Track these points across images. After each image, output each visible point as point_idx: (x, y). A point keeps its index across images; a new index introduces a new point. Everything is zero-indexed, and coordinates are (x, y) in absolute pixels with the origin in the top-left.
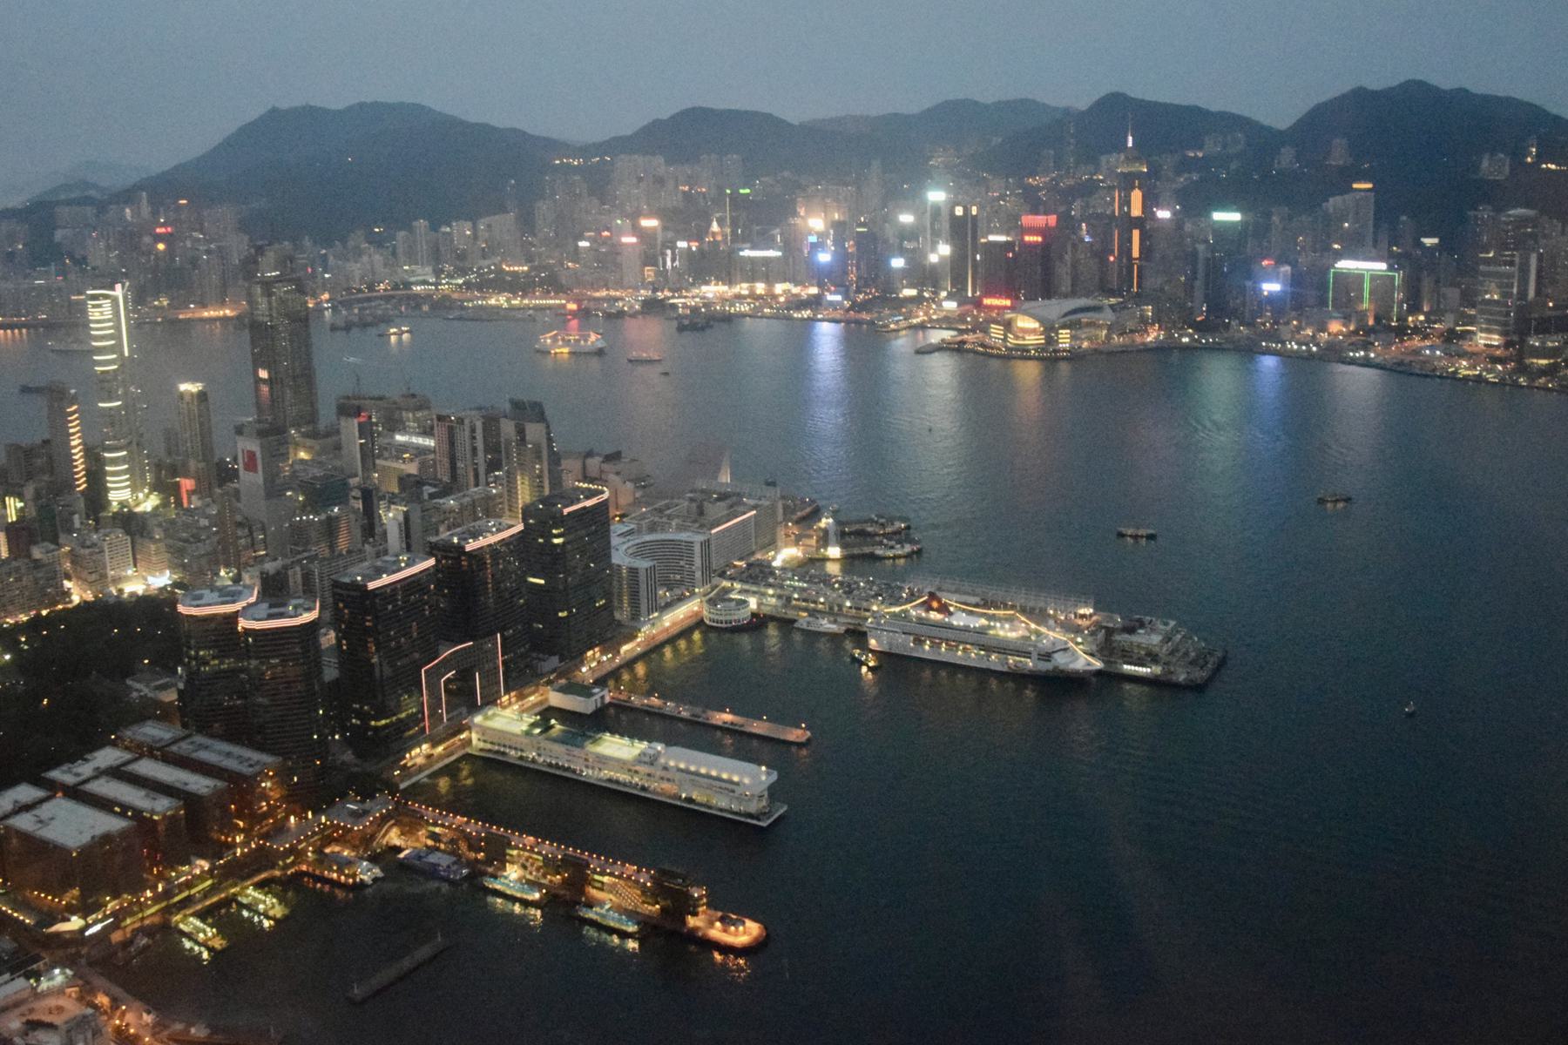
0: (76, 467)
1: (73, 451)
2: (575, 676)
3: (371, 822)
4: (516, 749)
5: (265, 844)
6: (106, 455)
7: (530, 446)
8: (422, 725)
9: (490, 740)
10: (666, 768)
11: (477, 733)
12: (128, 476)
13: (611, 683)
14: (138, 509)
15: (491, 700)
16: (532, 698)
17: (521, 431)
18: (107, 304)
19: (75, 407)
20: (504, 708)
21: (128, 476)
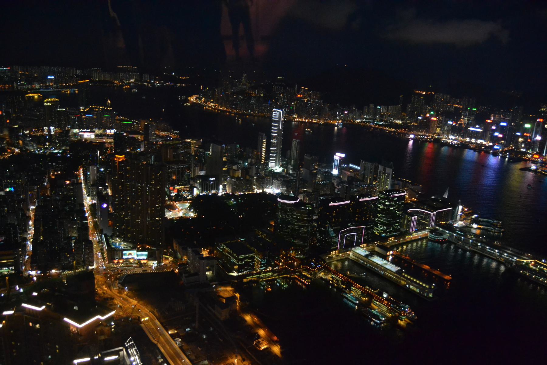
0: (263, 156)
1: (263, 152)
2: (385, 244)
3: (316, 269)
4: (362, 260)
5: (289, 268)
6: (270, 154)
7: (386, 175)
8: (337, 247)
9: (355, 255)
10: (404, 276)
11: (352, 253)
12: (275, 161)
13: (395, 249)
14: (275, 171)
15: (358, 245)
16: (370, 247)
17: (385, 170)
18: (278, 113)
19: (265, 140)
20: (361, 248)
21: (275, 161)
